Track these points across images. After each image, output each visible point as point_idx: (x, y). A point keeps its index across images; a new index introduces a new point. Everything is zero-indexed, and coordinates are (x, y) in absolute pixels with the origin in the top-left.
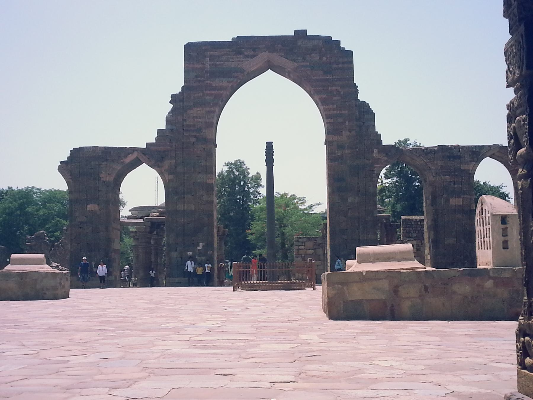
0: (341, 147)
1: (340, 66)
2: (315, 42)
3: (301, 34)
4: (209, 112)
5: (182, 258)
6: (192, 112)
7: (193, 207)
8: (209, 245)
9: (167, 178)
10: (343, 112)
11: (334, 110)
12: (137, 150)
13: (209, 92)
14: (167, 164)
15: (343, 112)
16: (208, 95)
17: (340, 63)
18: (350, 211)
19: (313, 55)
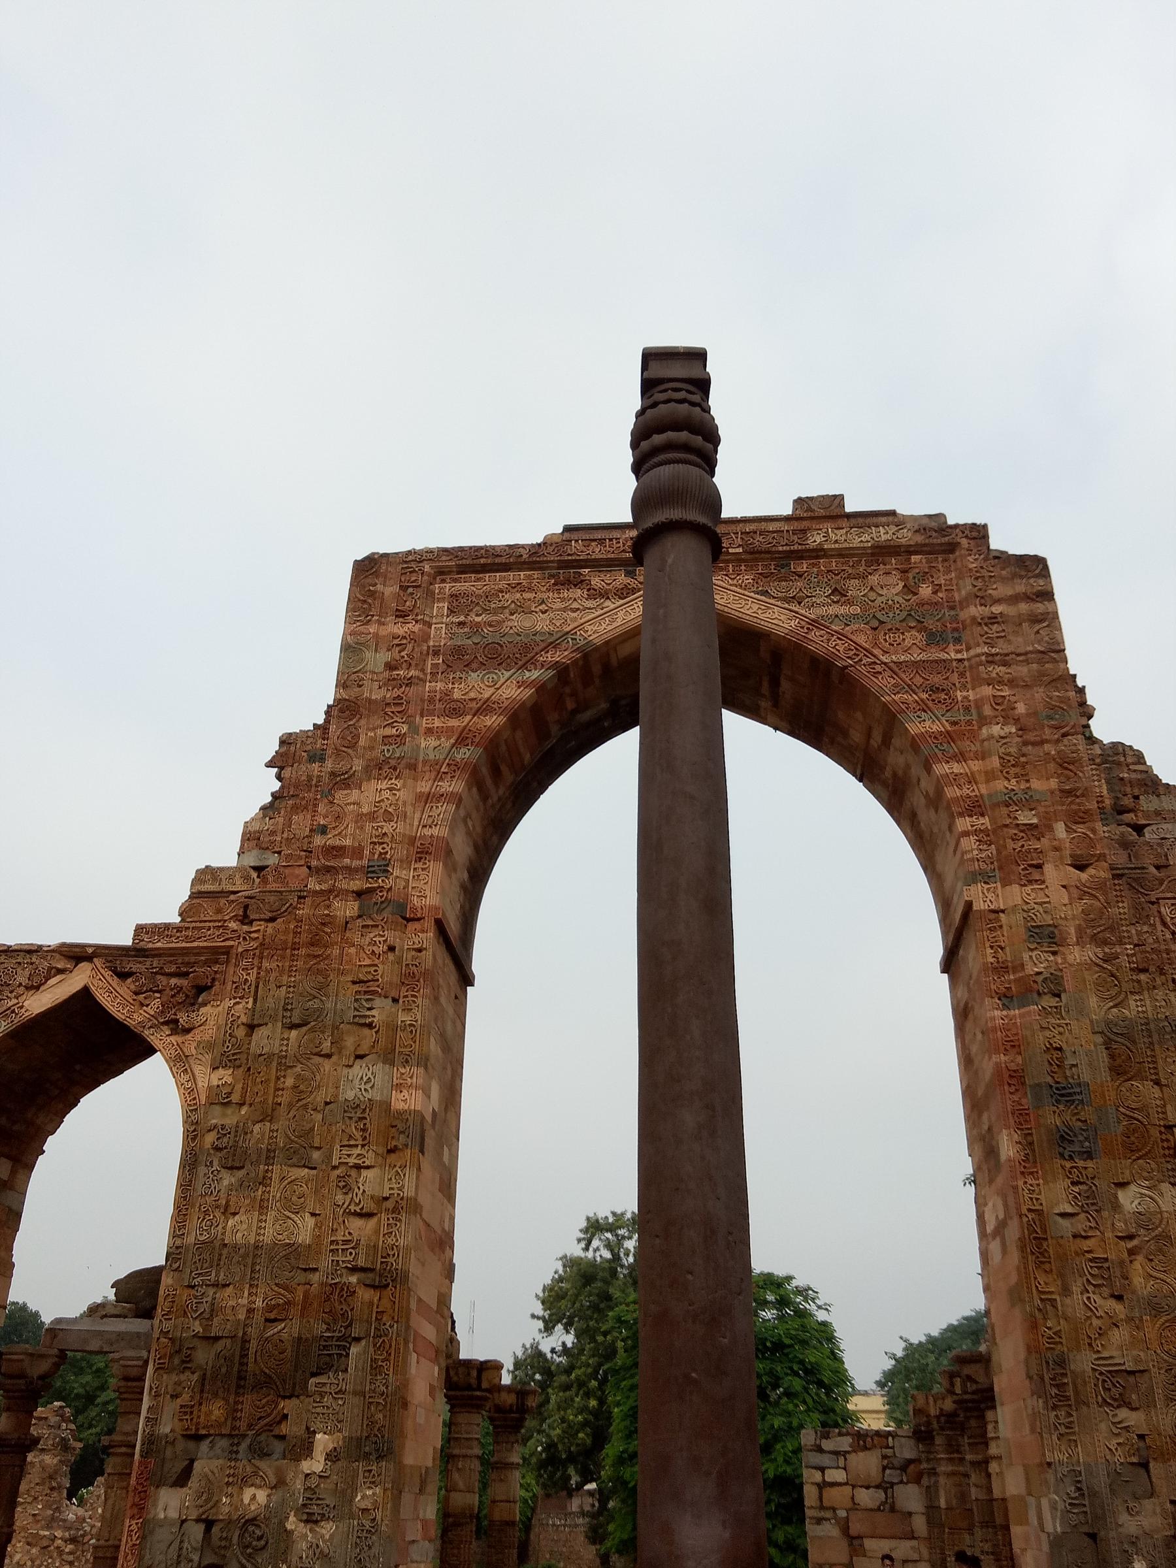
0: (1046, 936)
1: (997, 609)
2: (884, 535)
3: (822, 511)
4: (427, 799)
5: (209, 1524)
6: (355, 795)
7: (304, 1229)
8: (373, 1446)
9: (202, 1083)
10: (1036, 784)
11: (990, 776)
12: (89, 958)
13: (437, 723)
14: (212, 1016)
15: (1036, 784)
16: (429, 731)
17: (998, 601)
18: (1140, 1258)
19: (874, 579)
